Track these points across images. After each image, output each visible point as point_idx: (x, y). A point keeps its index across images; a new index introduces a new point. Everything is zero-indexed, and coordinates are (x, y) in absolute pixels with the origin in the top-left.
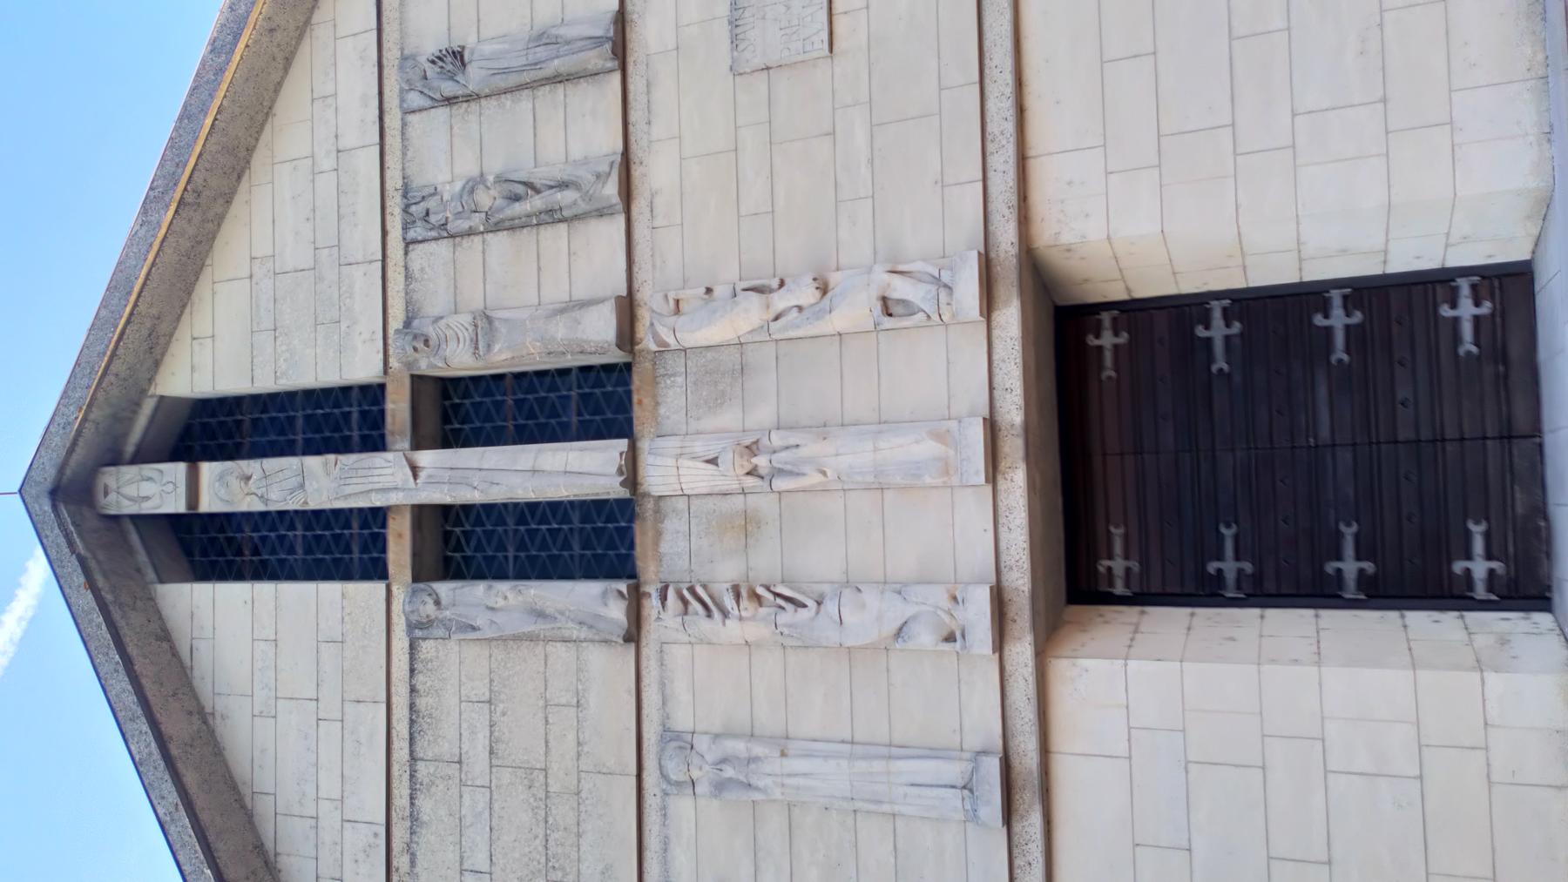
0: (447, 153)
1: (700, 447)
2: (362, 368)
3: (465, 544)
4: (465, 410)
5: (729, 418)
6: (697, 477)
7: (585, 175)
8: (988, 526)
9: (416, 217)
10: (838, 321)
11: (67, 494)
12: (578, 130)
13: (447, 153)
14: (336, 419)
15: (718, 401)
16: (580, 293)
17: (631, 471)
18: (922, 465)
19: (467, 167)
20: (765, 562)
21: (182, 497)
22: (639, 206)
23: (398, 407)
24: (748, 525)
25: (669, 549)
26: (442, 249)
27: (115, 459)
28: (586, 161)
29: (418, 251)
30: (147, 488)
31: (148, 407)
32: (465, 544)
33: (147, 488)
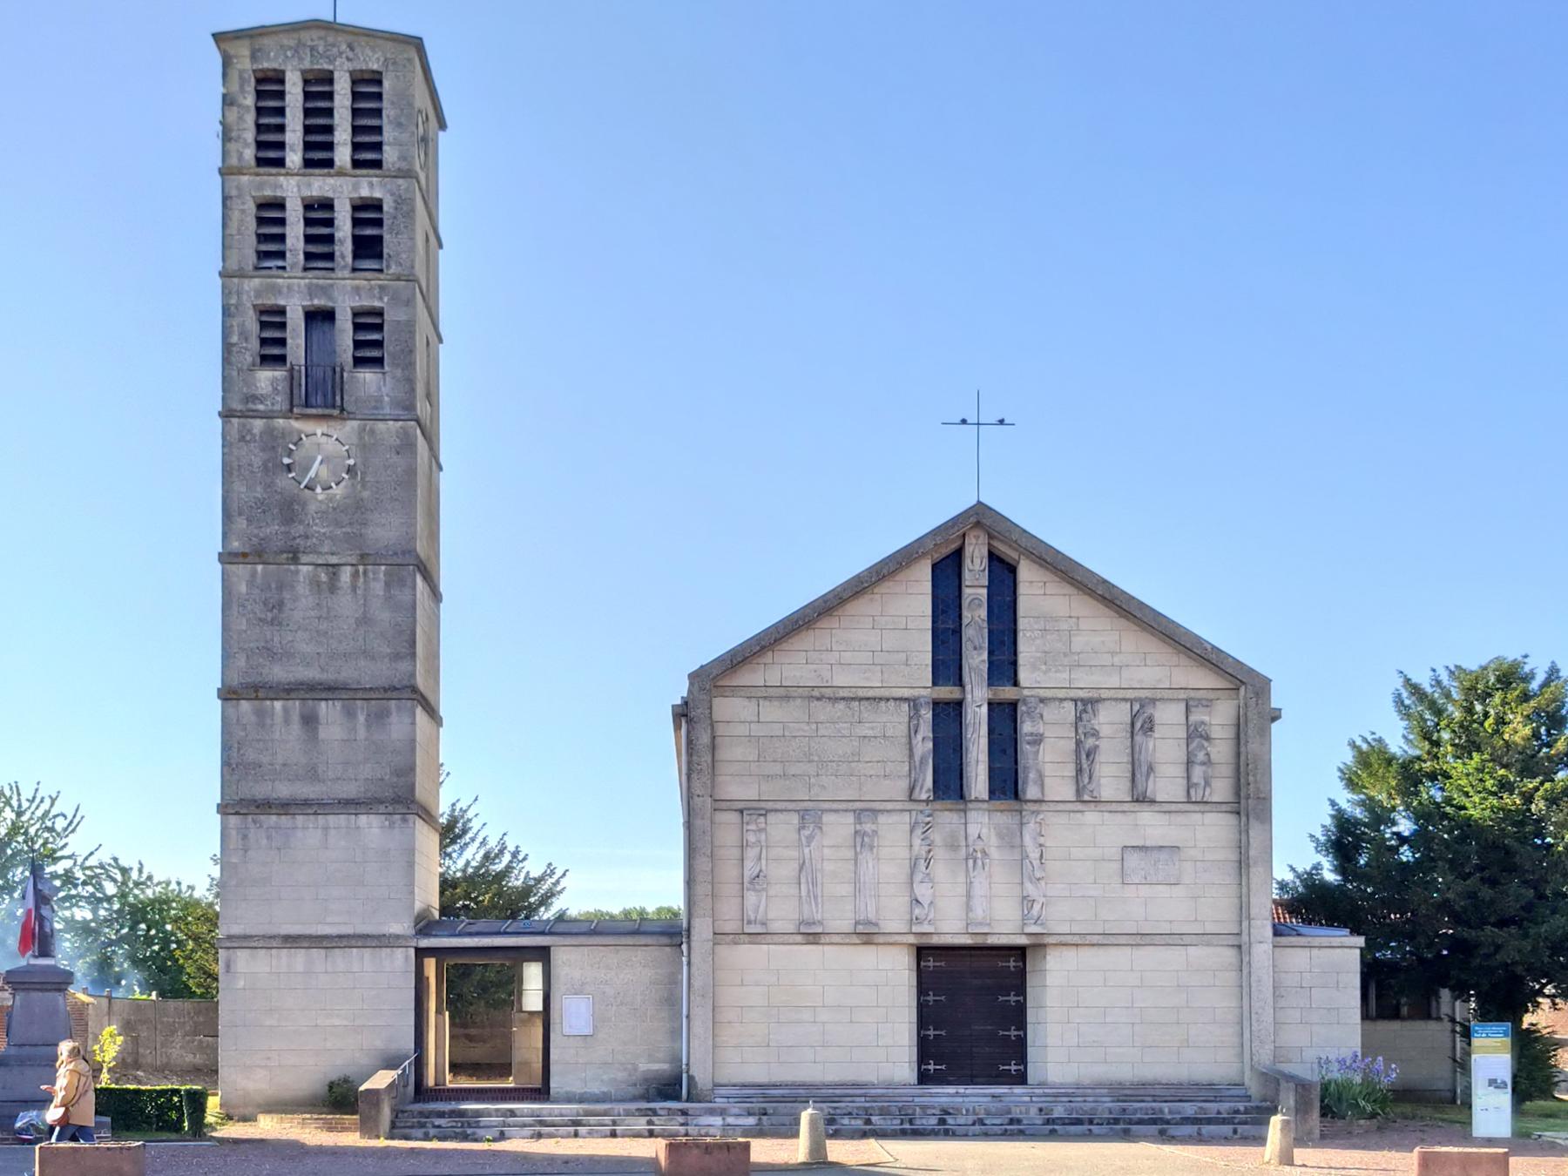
0: (1110, 720)
1: (985, 831)
2: (1024, 676)
3: (948, 715)
4: (1005, 716)
5: (994, 841)
6: (973, 830)
7: (1090, 787)
8: (951, 929)
9: (1086, 705)
10: (1028, 885)
11: (980, 518)
12: (1110, 780)
13: (1110, 720)
14: (1004, 666)
15: (1000, 836)
16: (1047, 781)
17: (977, 800)
18: (975, 903)
19: (1105, 731)
20: (940, 853)
21: (976, 579)
22: (1079, 806)
23: (1007, 693)
24: (953, 847)
25: (947, 819)
26: (1072, 718)
27: (991, 537)
28: (1099, 785)
29: (1071, 705)
30: (977, 561)
31: (1014, 555)
32: (948, 715)
33: (977, 561)
